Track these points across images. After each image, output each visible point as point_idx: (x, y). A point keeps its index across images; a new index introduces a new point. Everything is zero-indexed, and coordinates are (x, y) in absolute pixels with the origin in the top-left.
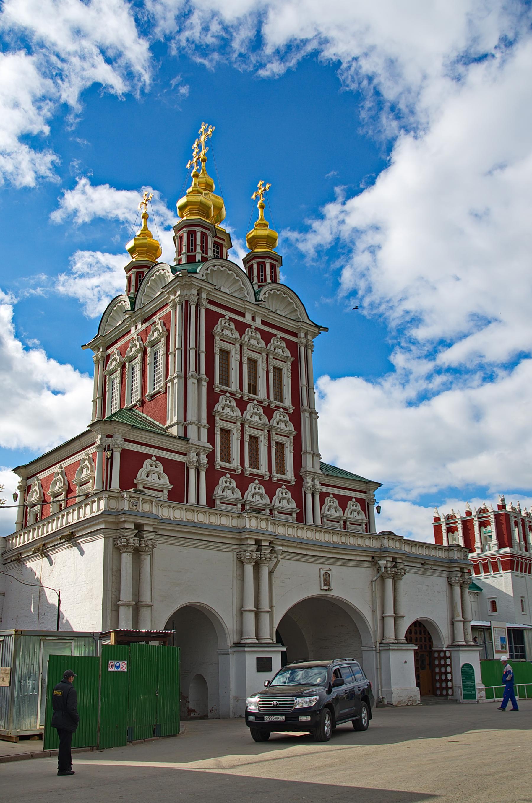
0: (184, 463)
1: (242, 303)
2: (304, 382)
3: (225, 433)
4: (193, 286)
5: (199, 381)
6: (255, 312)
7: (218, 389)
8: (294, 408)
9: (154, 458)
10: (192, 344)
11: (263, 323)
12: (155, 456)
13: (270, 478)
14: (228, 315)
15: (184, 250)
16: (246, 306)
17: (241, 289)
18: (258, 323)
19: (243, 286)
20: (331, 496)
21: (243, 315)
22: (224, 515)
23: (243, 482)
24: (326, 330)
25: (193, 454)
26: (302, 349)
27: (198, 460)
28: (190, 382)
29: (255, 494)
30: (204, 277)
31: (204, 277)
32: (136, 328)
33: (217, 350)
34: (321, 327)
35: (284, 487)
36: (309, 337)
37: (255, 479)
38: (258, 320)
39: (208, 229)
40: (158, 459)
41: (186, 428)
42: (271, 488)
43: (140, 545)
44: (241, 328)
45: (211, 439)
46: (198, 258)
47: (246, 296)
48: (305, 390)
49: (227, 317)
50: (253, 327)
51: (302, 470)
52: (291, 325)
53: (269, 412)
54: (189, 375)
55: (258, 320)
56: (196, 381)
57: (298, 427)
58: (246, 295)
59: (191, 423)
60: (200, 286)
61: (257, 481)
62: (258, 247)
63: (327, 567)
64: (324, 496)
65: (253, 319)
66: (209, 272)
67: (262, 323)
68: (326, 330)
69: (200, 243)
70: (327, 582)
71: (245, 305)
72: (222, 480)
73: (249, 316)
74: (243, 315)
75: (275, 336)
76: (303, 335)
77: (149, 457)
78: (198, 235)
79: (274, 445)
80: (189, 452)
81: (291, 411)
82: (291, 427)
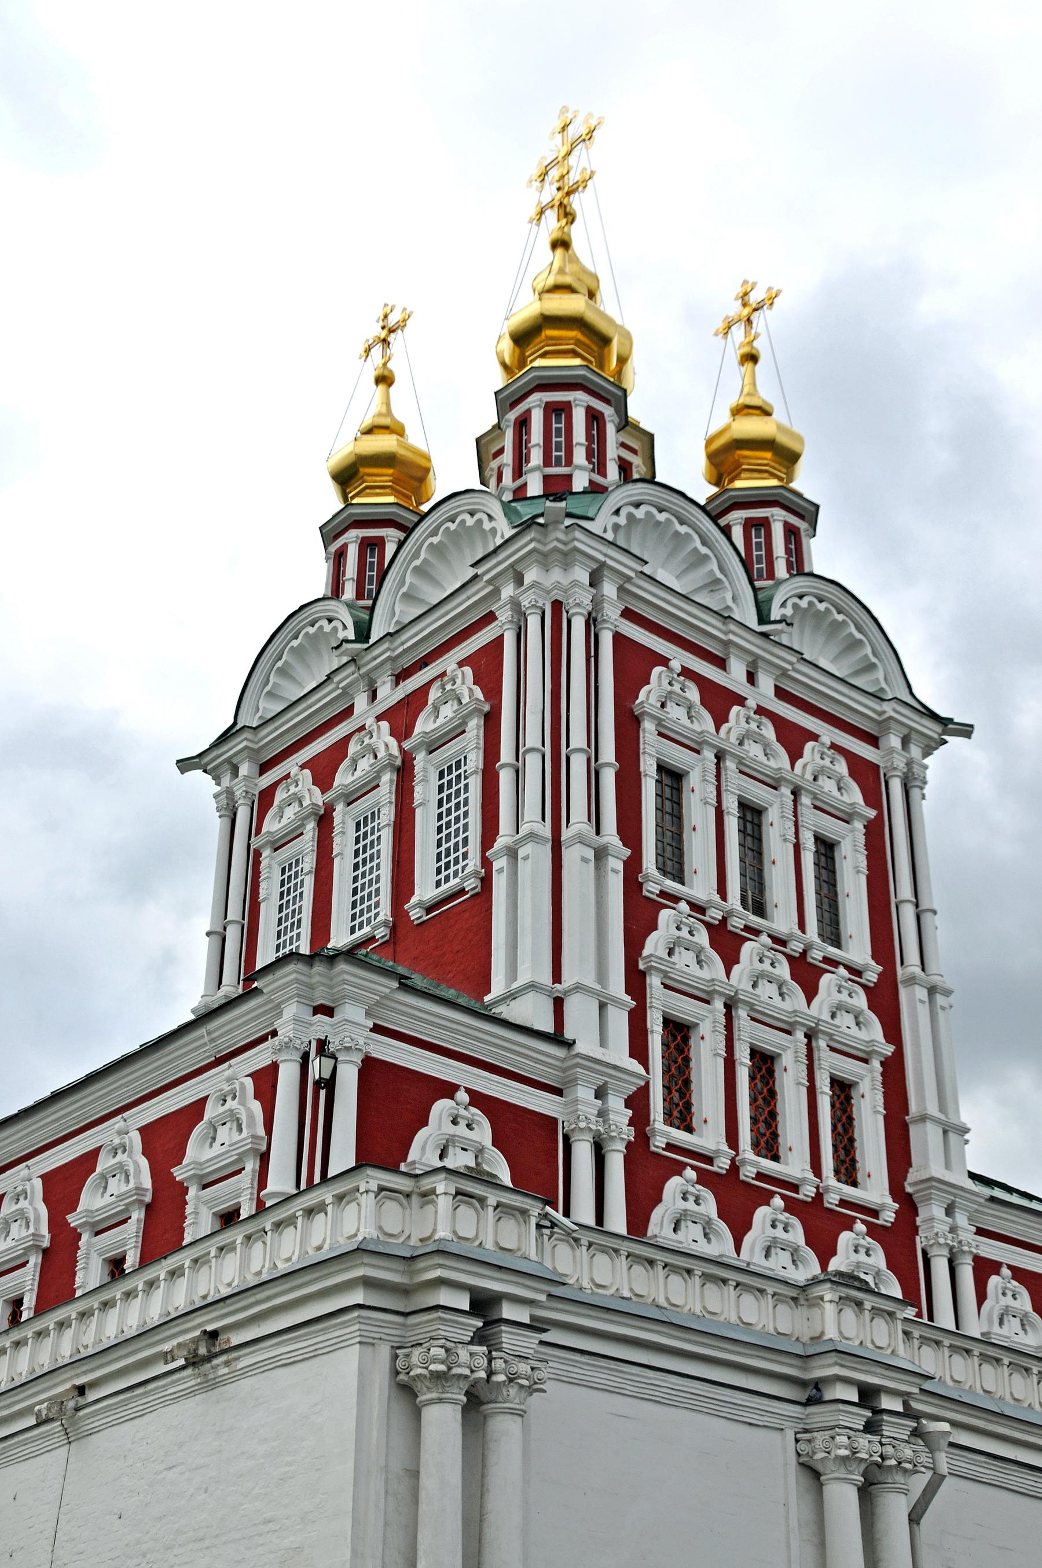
0: (555, 1121)
2: (905, 890)
3: (678, 1032)
4: (578, 557)
5: (601, 854)
7: (656, 889)
8: (880, 968)
9: (462, 1096)
10: (578, 738)
12: (468, 1091)
13: (819, 1196)
14: (680, 658)
15: (536, 457)
16: (732, 637)
19: (719, 575)
20: (1006, 1272)
21: (721, 663)
22: (748, 1288)
24: (966, 731)
25: (585, 1093)
26: (896, 786)
27: (602, 1114)
28: (571, 856)
32: (373, 696)
33: (648, 766)
34: (950, 720)
35: (860, 1227)
37: (772, 1194)
38: (766, 683)
40: (478, 1099)
41: (558, 1004)
42: (822, 1225)
43: (490, 1373)
44: (719, 702)
45: (639, 1050)
46: (580, 482)
47: (728, 608)
48: (908, 913)
49: (676, 665)
50: (751, 703)
51: (913, 1176)
52: (862, 709)
53: (806, 974)
54: (566, 834)
56: (590, 854)
57: (893, 1032)
58: (730, 603)
59: (578, 988)
60: (602, 558)
61: (778, 1202)
62: (743, 475)
64: (985, 1268)
65: (751, 678)
66: (622, 520)
67: (776, 695)
68: (966, 731)
69: (583, 440)
72: (673, 1185)
76: (895, 742)
77: (448, 1090)
78: (579, 417)
80: (573, 1082)
81: (872, 977)
82: (875, 1031)
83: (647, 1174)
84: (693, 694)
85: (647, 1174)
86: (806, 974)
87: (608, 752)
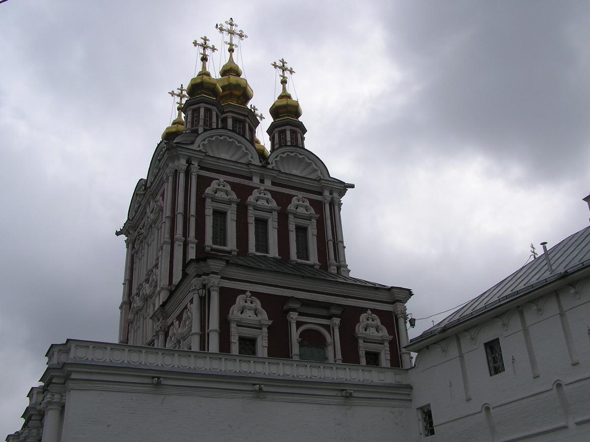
1: (246, 167)
6: (263, 174)
11: (273, 184)
16: (251, 170)
18: (268, 183)
26: (327, 206)
30: (201, 148)
31: (201, 148)
36: (336, 195)
39: (213, 105)
50: (262, 188)
58: (250, 159)
65: (262, 181)
67: (272, 185)
71: (249, 169)
73: (256, 180)
76: (326, 193)
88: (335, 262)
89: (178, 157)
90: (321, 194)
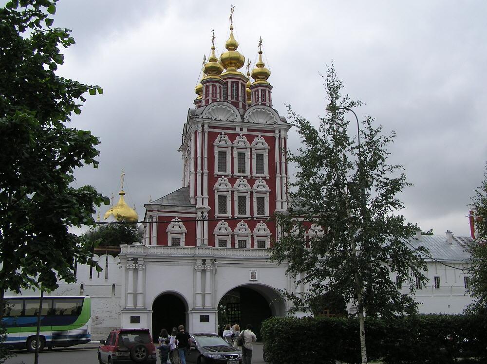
5: (203, 174)
11: (248, 130)
17: (233, 115)
23: (233, 222)
29: (242, 229)
36: (282, 132)
38: (245, 130)
40: (179, 218)
44: (232, 137)
45: (211, 202)
50: (241, 135)
52: (269, 128)
53: (251, 181)
55: (245, 130)
58: (236, 117)
63: (253, 269)
65: (241, 130)
70: (253, 276)
74: (234, 129)
75: (257, 136)
76: (277, 132)
77: (174, 217)
79: (255, 200)
83: (213, 222)
84: (227, 138)
85: (213, 222)
86: (251, 181)
87: (206, 155)
88: (279, 174)
89: (197, 122)
90: (273, 132)
